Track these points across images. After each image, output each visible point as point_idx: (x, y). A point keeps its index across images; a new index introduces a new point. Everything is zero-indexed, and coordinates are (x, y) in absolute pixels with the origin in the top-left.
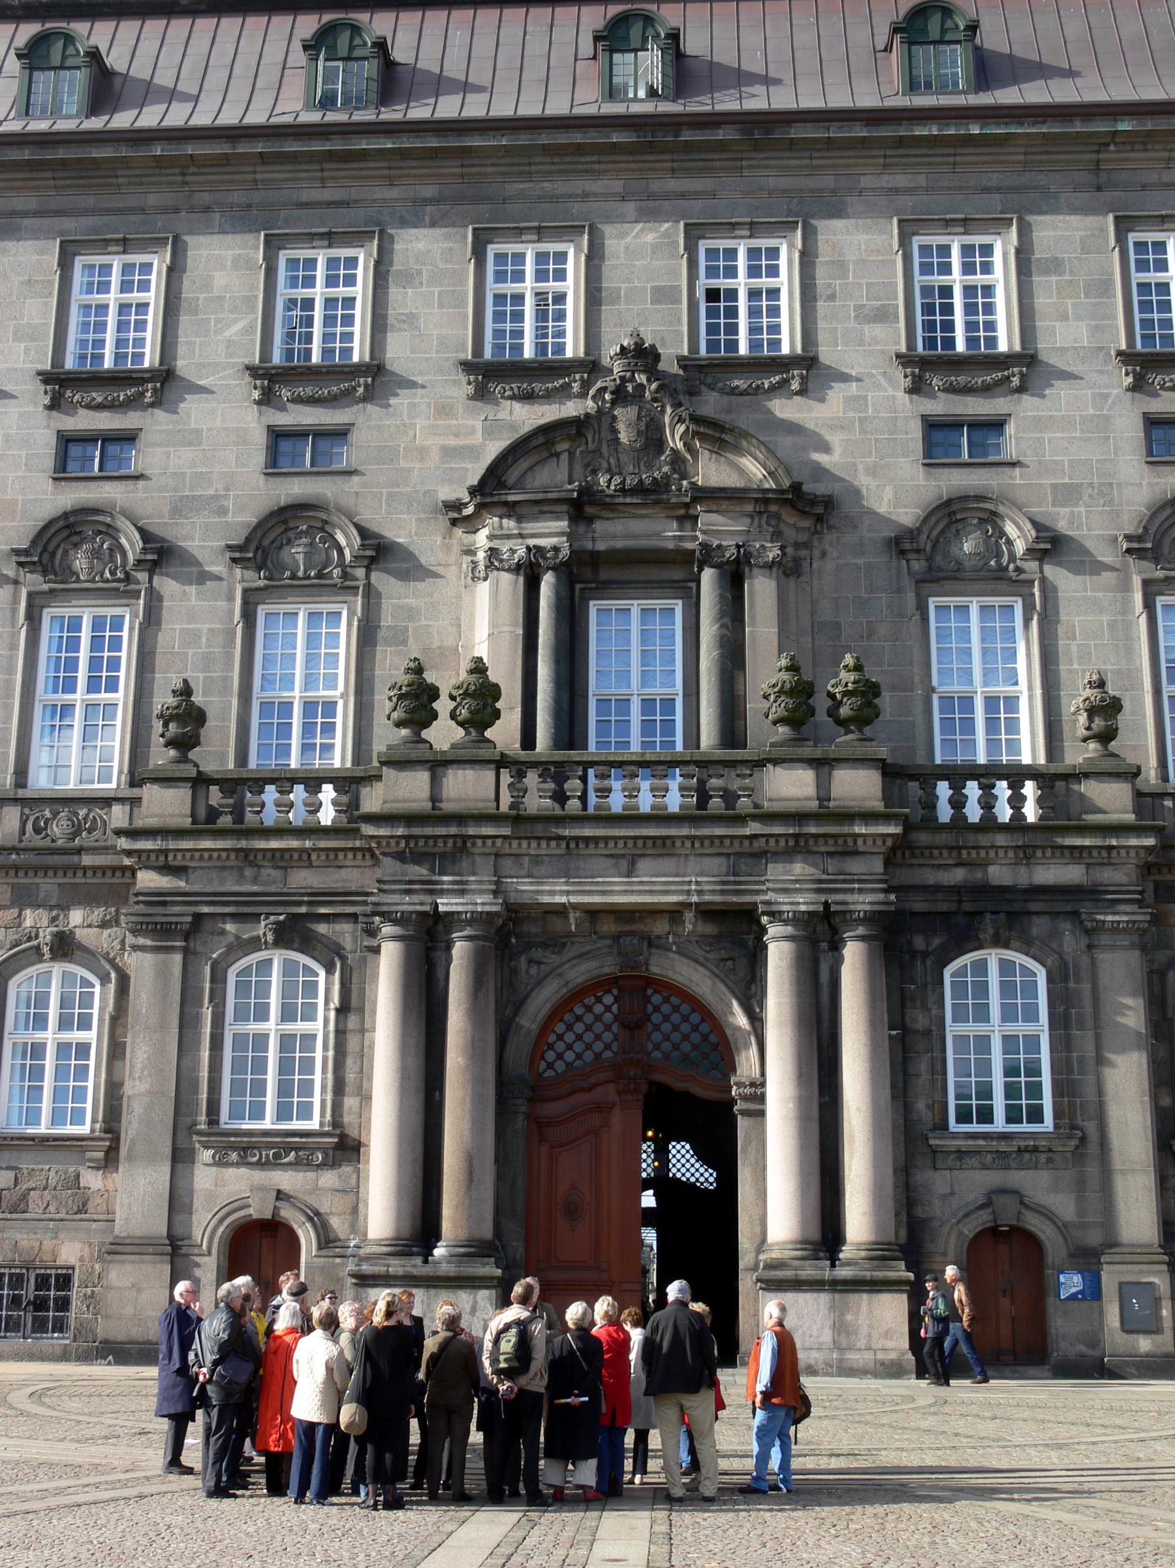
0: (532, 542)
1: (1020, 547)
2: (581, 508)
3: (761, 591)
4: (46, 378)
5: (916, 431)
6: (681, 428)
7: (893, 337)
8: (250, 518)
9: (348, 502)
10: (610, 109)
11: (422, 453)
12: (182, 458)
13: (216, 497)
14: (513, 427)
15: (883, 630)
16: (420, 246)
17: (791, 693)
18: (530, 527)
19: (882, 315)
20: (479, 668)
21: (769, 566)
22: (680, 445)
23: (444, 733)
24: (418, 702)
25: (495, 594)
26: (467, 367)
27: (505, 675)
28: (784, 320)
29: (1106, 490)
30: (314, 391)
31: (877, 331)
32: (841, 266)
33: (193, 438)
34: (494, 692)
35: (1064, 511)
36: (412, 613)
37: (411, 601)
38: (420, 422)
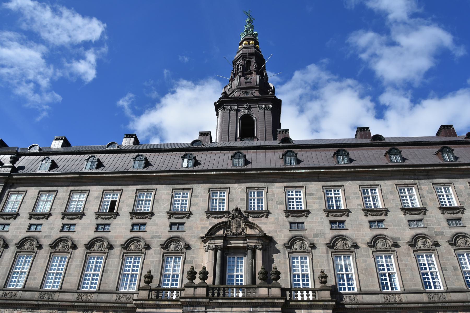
0: (216, 244)
2: (226, 238)
4: (131, 213)
5: (288, 224)
6: (244, 224)
7: (283, 207)
8: (165, 239)
9: (183, 237)
10: (233, 168)
11: (198, 227)
12: (154, 228)
13: (159, 235)
14: (214, 223)
15: (282, 261)
16: (199, 191)
17: (263, 274)
18: (216, 241)
19: (281, 203)
20: (204, 268)
21: (260, 249)
23: (197, 281)
24: (192, 275)
26: (206, 212)
27: (210, 269)
29: (323, 235)
30: (178, 216)
32: (274, 195)
33: (156, 224)
34: (207, 273)
35: (315, 239)
36: (194, 258)
37: (194, 256)
38: (197, 222)
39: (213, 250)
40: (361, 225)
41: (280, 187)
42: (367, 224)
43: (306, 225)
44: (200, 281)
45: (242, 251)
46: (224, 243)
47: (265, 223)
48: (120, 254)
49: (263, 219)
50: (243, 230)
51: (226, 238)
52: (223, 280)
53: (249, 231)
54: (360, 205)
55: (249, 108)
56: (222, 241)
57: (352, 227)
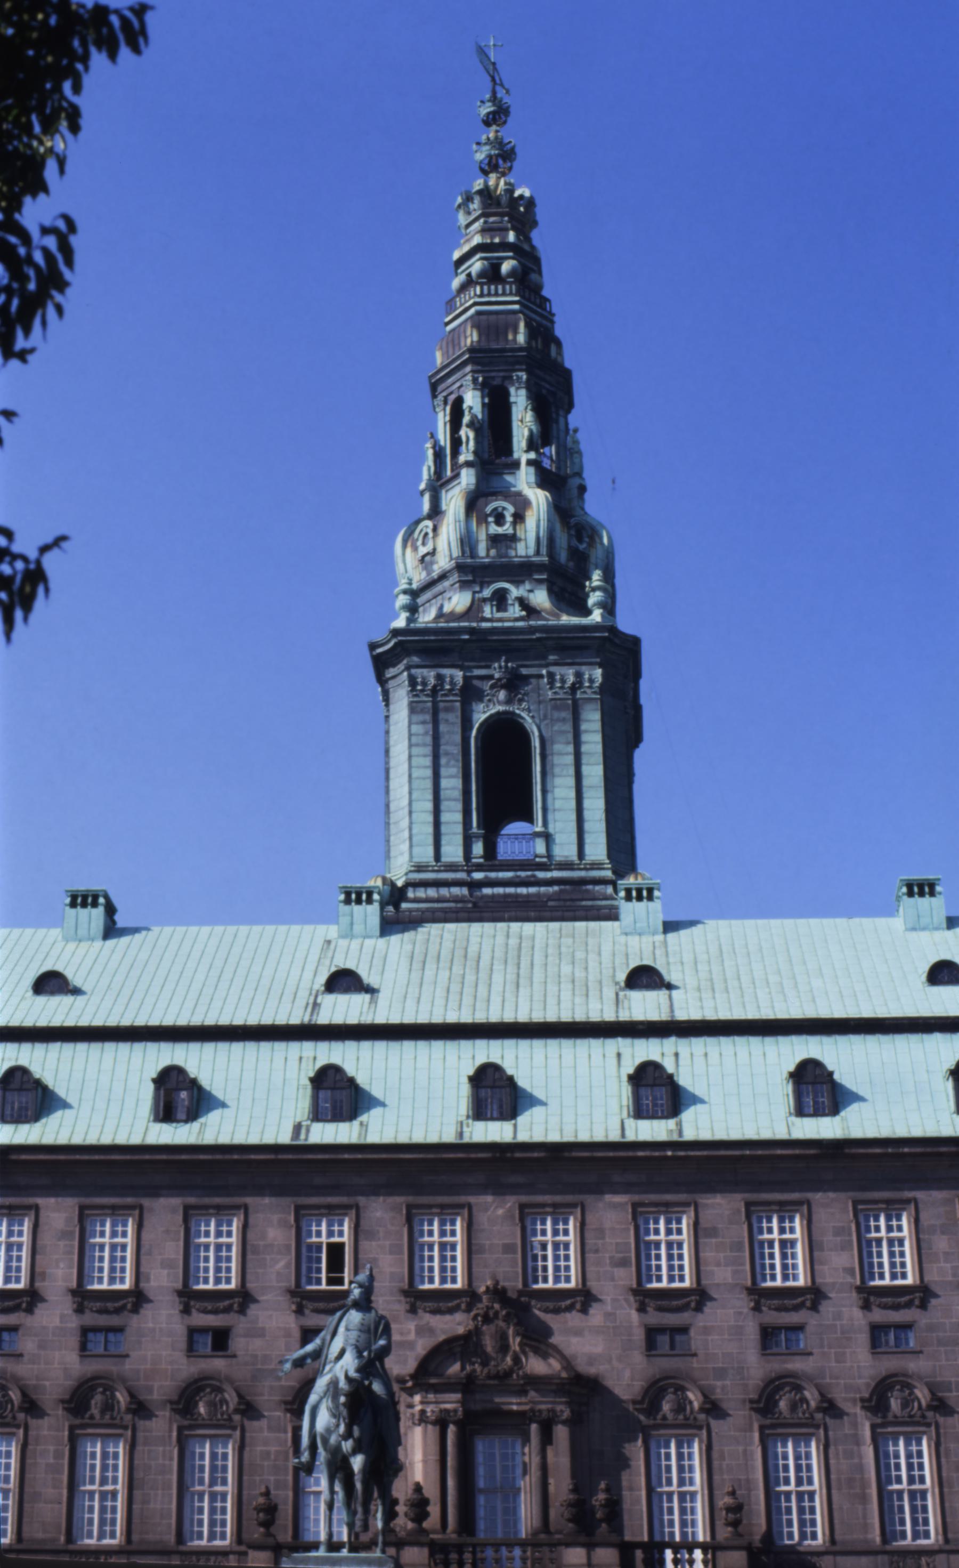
1: (696, 1405)
2: (467, 1386)
3: (561, 1433)
4: (180, 1294)
6: (518, 1339)
12: (256, 1344)
14: (431, 1331)
19: (624, 1263)
21: (564, 1422)
22: (517, 1348)
25: (425, 1433)
27: (431, 1492)
28: (572, 1263)
31: (620, 1272)
32: (601, 1232)
35: (719, 1383)
39: (434, 1423)
40: (849, 1339)
41: (621, 1205)
42: (863, 1338)
43: (696, 1339)
44: (410, 1525)
45: (516, 1424)
46: (463, 1402)
47: (578, 1332)
48: (170, 1431)
49: (573, 1319)
50: (517, 1360)
51: (467, 1386)
52: (467, 1521)
53: (536, 1365)
54: (851, 1271)
55: (514, 684)
56: (458, 1396)
57: (822, 1346)
